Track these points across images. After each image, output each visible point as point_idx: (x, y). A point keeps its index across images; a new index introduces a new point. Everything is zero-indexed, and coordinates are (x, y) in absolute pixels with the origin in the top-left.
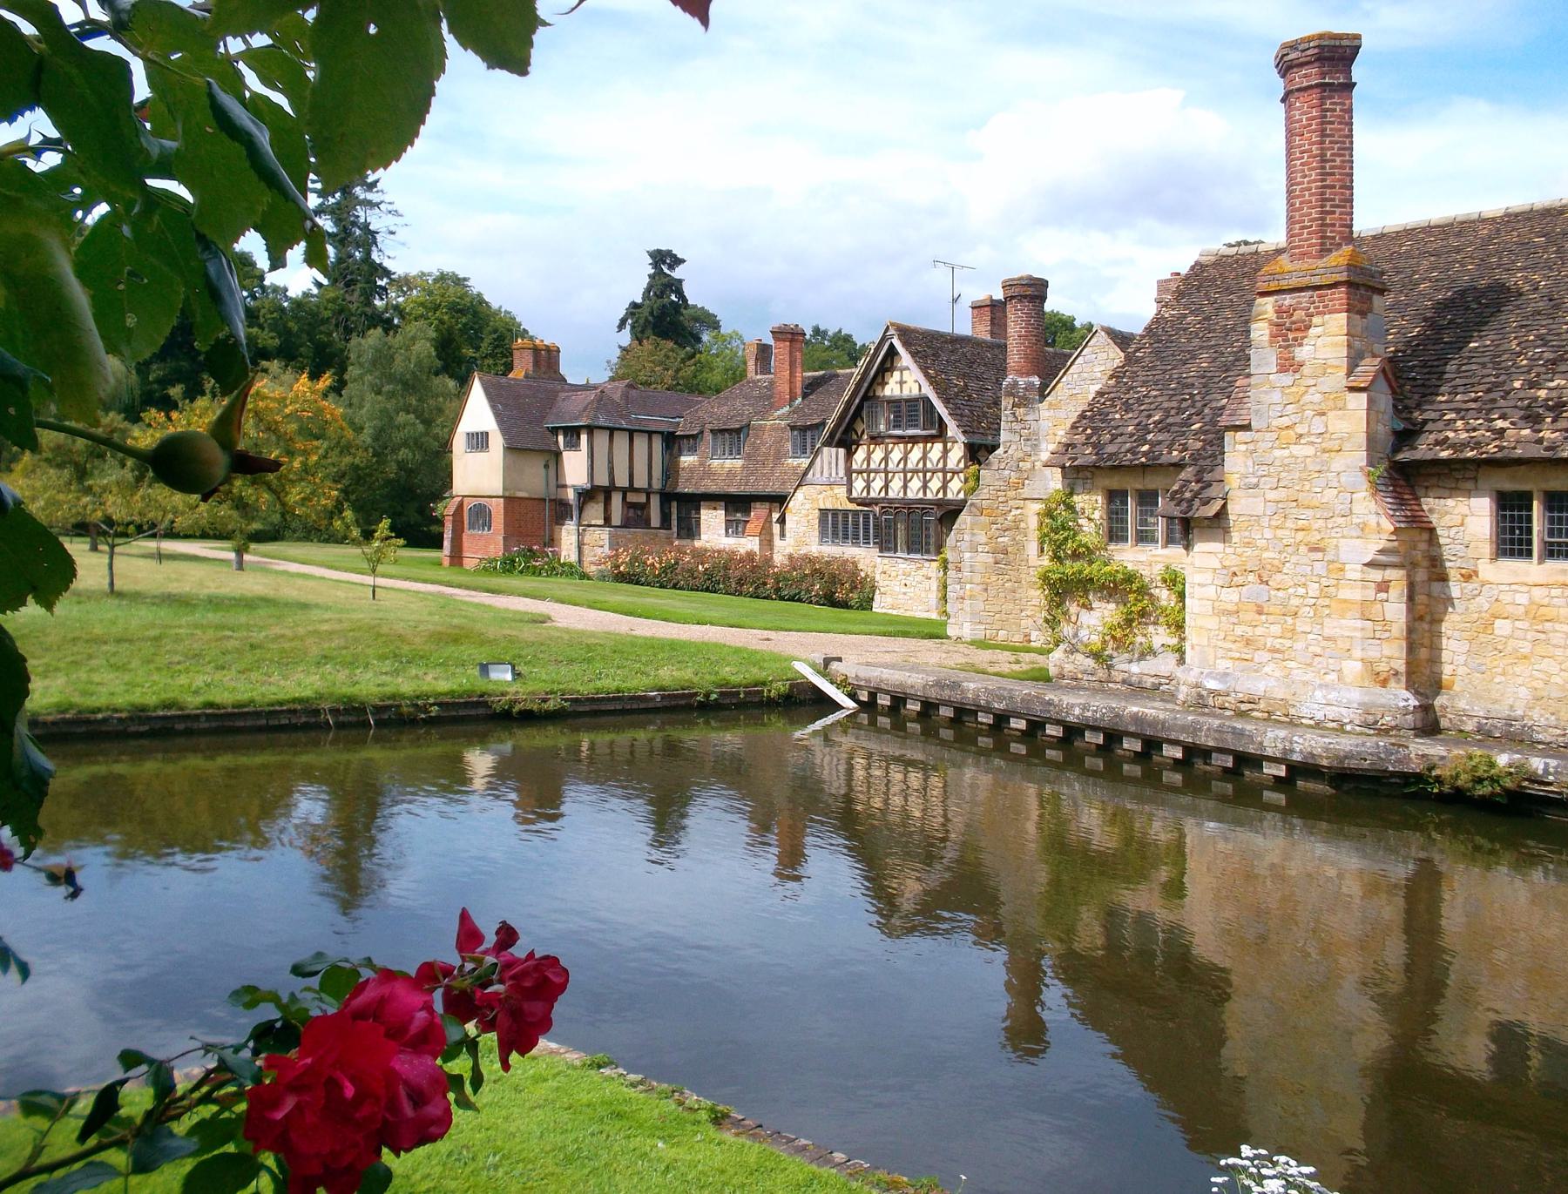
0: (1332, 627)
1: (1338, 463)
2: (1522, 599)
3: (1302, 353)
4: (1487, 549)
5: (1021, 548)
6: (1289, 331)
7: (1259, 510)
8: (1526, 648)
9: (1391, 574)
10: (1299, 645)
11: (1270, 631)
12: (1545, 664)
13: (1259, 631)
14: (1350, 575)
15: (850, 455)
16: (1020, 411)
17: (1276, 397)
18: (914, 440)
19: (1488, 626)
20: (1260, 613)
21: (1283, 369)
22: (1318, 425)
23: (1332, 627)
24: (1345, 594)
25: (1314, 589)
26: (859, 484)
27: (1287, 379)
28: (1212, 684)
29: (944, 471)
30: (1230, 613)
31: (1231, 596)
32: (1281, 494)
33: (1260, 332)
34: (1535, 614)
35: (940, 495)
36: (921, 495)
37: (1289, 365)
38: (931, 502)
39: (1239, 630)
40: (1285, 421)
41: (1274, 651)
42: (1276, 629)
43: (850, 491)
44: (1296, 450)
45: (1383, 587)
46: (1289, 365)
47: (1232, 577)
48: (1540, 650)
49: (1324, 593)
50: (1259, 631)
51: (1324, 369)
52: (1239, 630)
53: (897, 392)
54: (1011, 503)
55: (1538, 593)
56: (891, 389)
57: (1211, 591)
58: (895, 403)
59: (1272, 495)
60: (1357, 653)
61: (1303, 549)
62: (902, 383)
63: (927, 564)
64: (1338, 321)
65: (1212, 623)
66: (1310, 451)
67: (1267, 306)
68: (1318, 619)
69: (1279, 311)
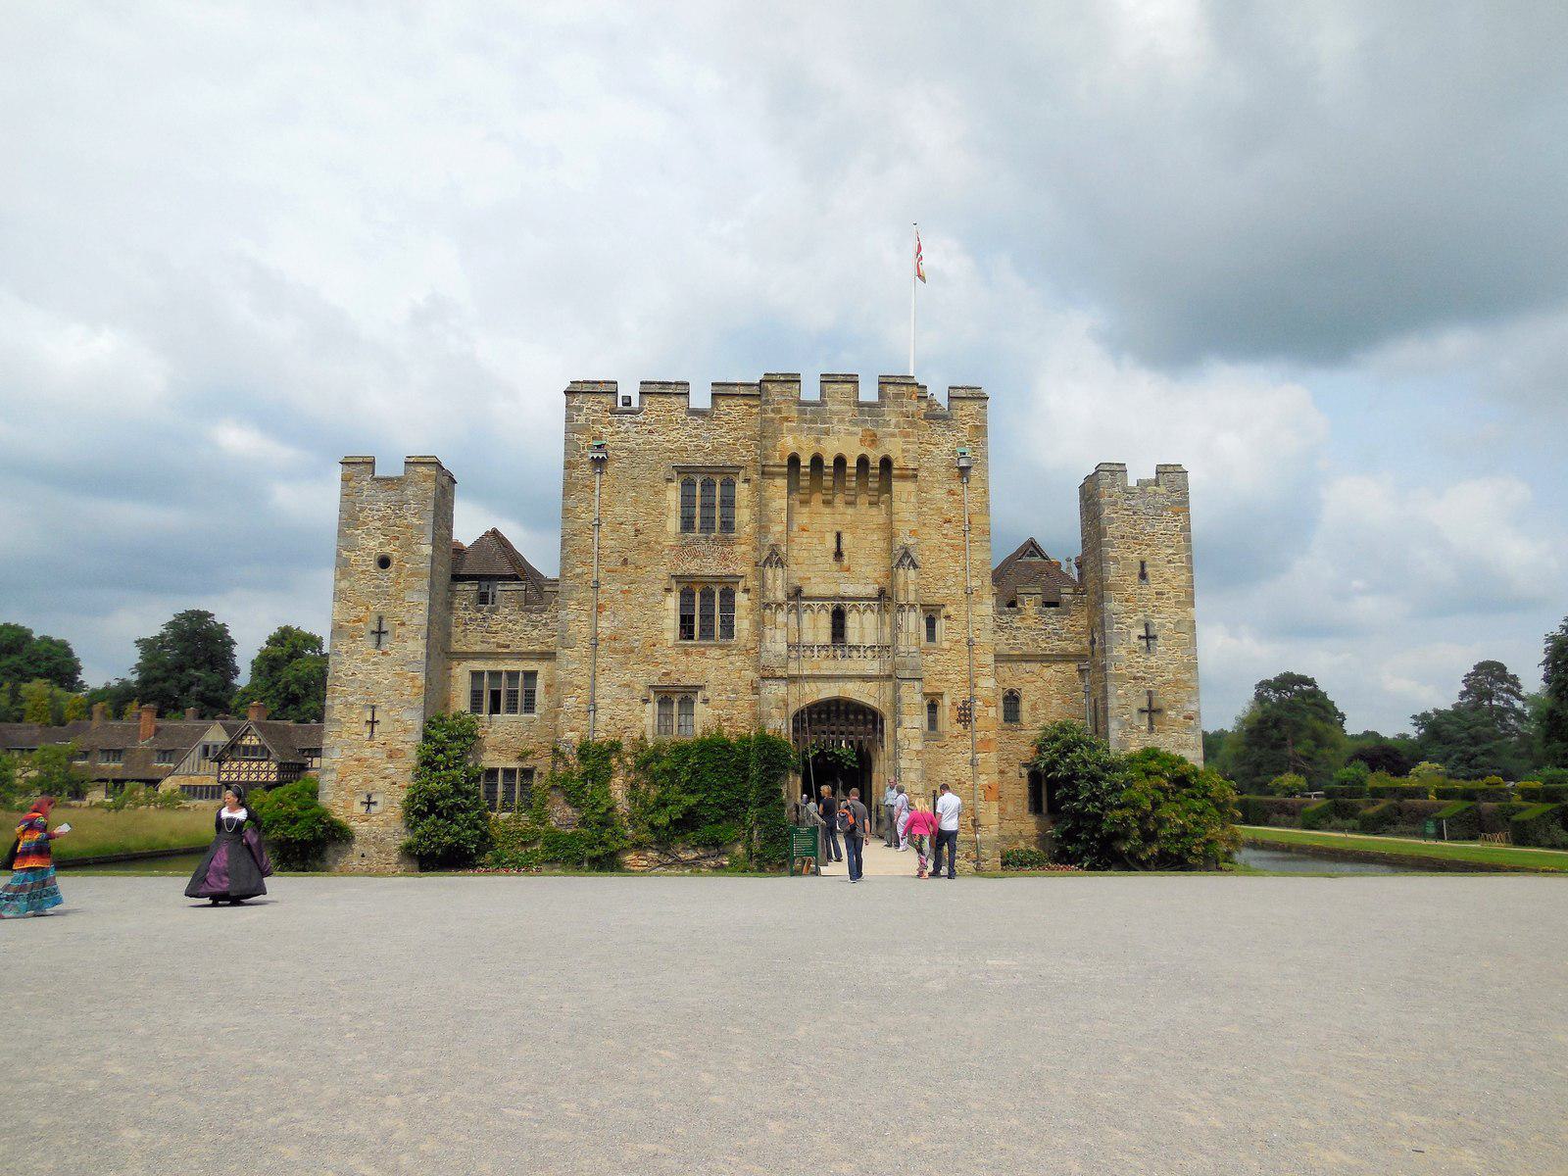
15: (220, 765)
18: (254, 760)
26: (224, 776)
56: (246, 741)
58: (246, 748)
62: (251, 740)
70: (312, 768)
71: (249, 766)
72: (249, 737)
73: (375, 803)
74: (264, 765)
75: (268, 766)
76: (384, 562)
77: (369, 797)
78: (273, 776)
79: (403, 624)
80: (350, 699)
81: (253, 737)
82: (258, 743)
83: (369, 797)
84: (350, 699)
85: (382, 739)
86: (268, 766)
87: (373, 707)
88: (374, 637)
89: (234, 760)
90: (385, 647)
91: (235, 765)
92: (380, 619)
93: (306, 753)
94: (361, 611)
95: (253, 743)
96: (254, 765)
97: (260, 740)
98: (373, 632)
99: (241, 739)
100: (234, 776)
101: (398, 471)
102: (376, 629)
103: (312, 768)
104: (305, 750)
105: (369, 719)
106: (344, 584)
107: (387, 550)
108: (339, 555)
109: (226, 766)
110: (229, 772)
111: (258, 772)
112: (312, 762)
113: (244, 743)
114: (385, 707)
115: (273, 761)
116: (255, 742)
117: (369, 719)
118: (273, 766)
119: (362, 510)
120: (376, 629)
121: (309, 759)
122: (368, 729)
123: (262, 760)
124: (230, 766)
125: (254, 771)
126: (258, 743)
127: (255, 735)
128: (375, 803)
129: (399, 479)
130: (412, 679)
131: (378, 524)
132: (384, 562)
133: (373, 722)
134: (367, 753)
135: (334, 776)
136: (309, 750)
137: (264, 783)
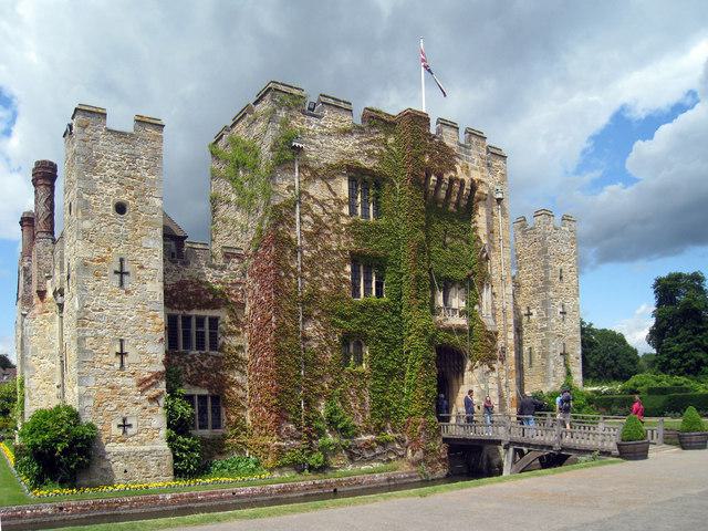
73: (130, 426)
76: (121, 208)
77: (124, 420)
79: (142, 267)
80: (100, 332)
83: (124, 420)
84: (100, 332)
85: (131, 369)
87: (121, 341)
88: (118, 277)
90: (128, 286)
92: (122, 260)
94: (103, 251)
98: (116, 272)
101: (129, 127)
102: (118, 269)
105: (119, 351)
106: (87, 225)
107: (124, 198)
108: (80, 197)
114: (133, 341)
117: (119, 351)
119: (98, 157)
120: (118, 269)
122: (118, 360)
128: (130, 426)
129: (131, 135)
130: (154, 317)
131: (113, 172)
132: (121, 208)
133: (122, 354)
134: (120, 381)
135: (91, 402)
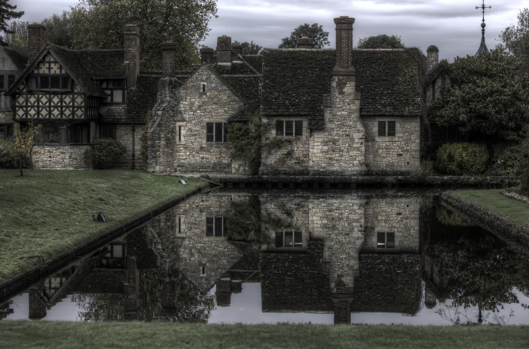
0: (351, 153)
1: (353, 116)
2: (384, 145)
3: (345, 90)
4: (377, 134)
5: (174, 138)
6: (341, 85)
7: (334, 126)
8: (385, 155)
9: (363, 140)
10: (343, 158)
11: (336, 156)
12: (389, 158)
13: (333, 156)
14: (356, 141)
16: (174, 90)
17: (338, 100)
18: (55, 94)
19: (377, 151)
20: (333, 151)
21: (339, 94)
22: (348, 107)
23: (351, 153)
24: (355, 145)
25: (347, 145)
26: (21, 112)
27: (341, 96)
28: (322, 170)
29: (73, 107)
30: (325, 152)
31: (326, 148)
32: (339, 123)
33: (334, 84)
34: (387, 148)
35: (71, 117)
36: (59, 117)
37: (341, 93)
38: (65, 120)
39: (328, 156)
40: (340, 106)
41: (337, 160)
42: (337, 155)
43: (14, 115)
44: (343, 113)
45: (361, 144)
46: (341, 93)
47: (325, 143)
48: (388, 155)
49: (350, 146)
50: (333, 156)
51: (350, 94)
52: (328, 156)
53: (47, 71)
54: (171, 122)
55: (387, 143)
56: (44, 70)
57: (320, 147)
59: (336, 123)
60: (357, 159)
61: (344, 136)
62: (50, 68)
63: (62, 147)
64: (353, 84)
65: (321, 155)
66: (346, 113)
67: (336, 79)
68: (348, 152)
69: (339, 80)
70: (112, 103)
71: (50, 101)
72: (47, 65)
74: (67, 100)
75: (73, 100)
78: (79, 113)
81: (52, 65)
82: (58, 72)
86: (73, 100)
89: (31, 92)
91: (32, 100)
93: (104, 86)
95: (52, 72)
96: (56, 100)
97: (61, 68)
99: (38, 68)
100: (32, 112)
103: (112, 103)
104: (102, 82)
109: (21, 100)
110: (26, 107)
111: (61, 107)
112: (112, 95)
113: (41, 72)
115: (79, 94)
116: (55, 70)
118: (79, 100)
121: (108, 92)
123: (62, 94)
124: (27, 101)
125: (56, 107)
126: (58, 72)
127: (55, 62)
136: (108, 81)
137: (69, 121)
